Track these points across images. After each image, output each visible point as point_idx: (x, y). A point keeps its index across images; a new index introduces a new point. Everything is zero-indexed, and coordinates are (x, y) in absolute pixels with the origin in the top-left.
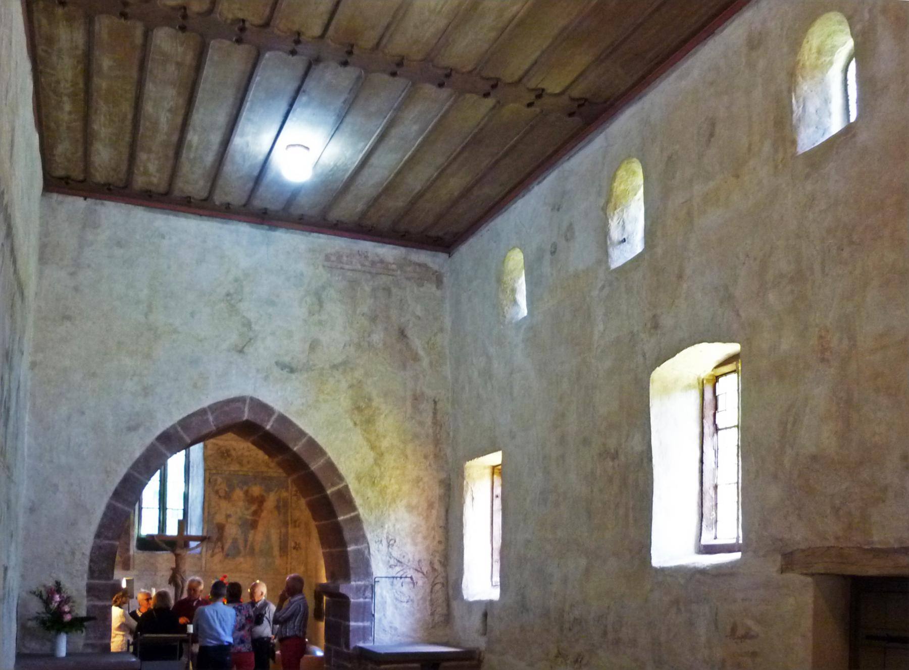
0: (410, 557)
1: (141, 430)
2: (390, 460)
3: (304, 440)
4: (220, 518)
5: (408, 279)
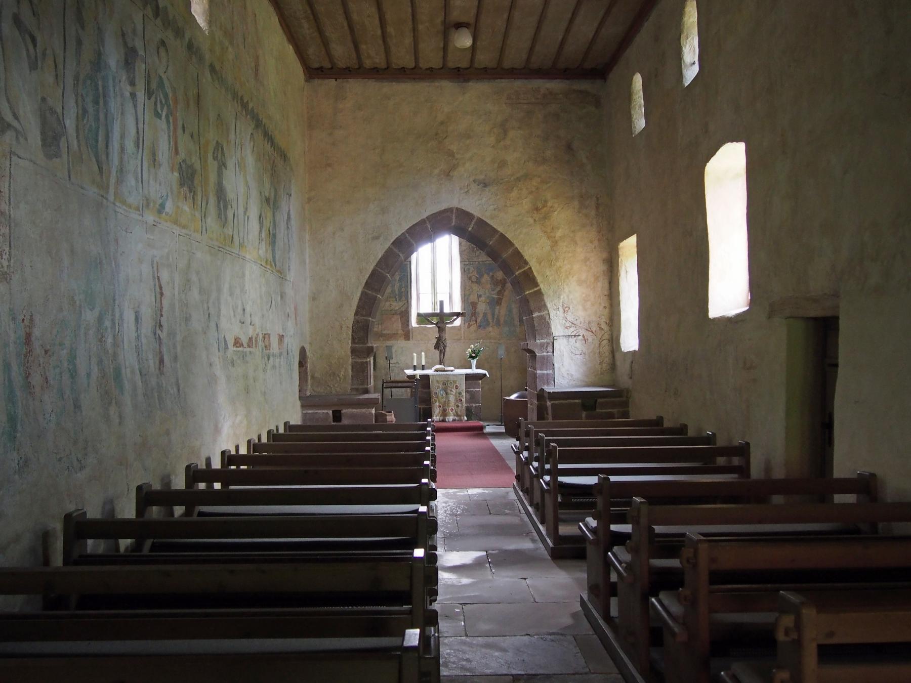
0: (581, 319)
1: (381, 238)
4: (473, 298)
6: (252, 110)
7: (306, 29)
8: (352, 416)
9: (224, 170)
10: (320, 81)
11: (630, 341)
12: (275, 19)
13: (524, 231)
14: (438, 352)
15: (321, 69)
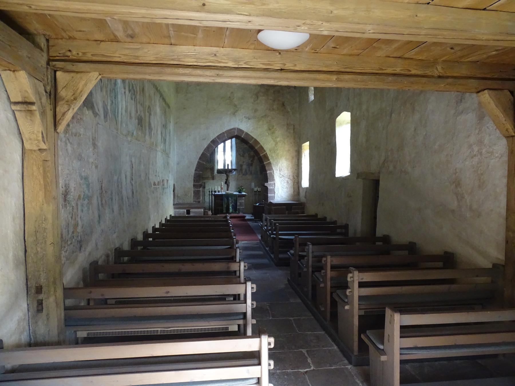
2: (280, 145)
4: (241, 163)
11: (305, 183)
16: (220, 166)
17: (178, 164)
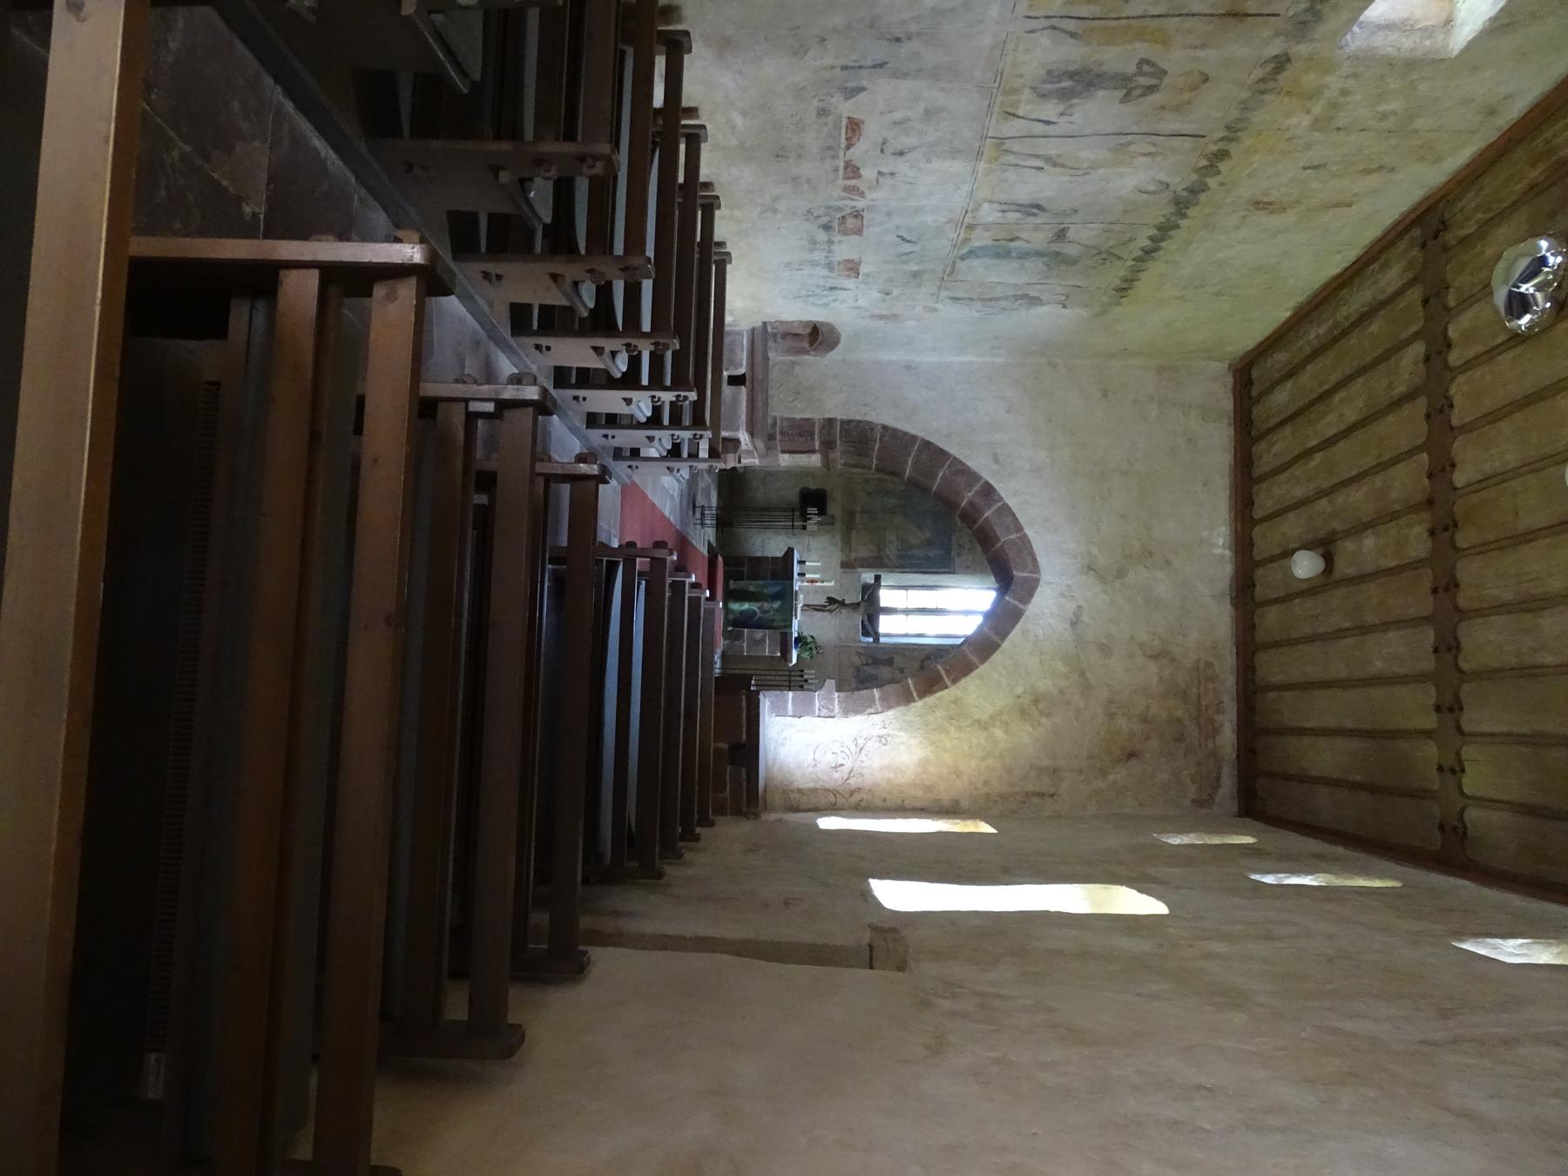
1: (996, 467)
2: (979, 738)
3: (995, 638)
4: (898, 660)
5: (1199, 764)
6: (1204, 188)
7: (1317, 332)
8: (735, 401)
9: (1120, 93)
10: (1230, 386)
12: (1335, 265)
13: (1004, 681)
14: (823, 601)
15: (1250, 382)
16: (886, 597)
17: (909, 367)
